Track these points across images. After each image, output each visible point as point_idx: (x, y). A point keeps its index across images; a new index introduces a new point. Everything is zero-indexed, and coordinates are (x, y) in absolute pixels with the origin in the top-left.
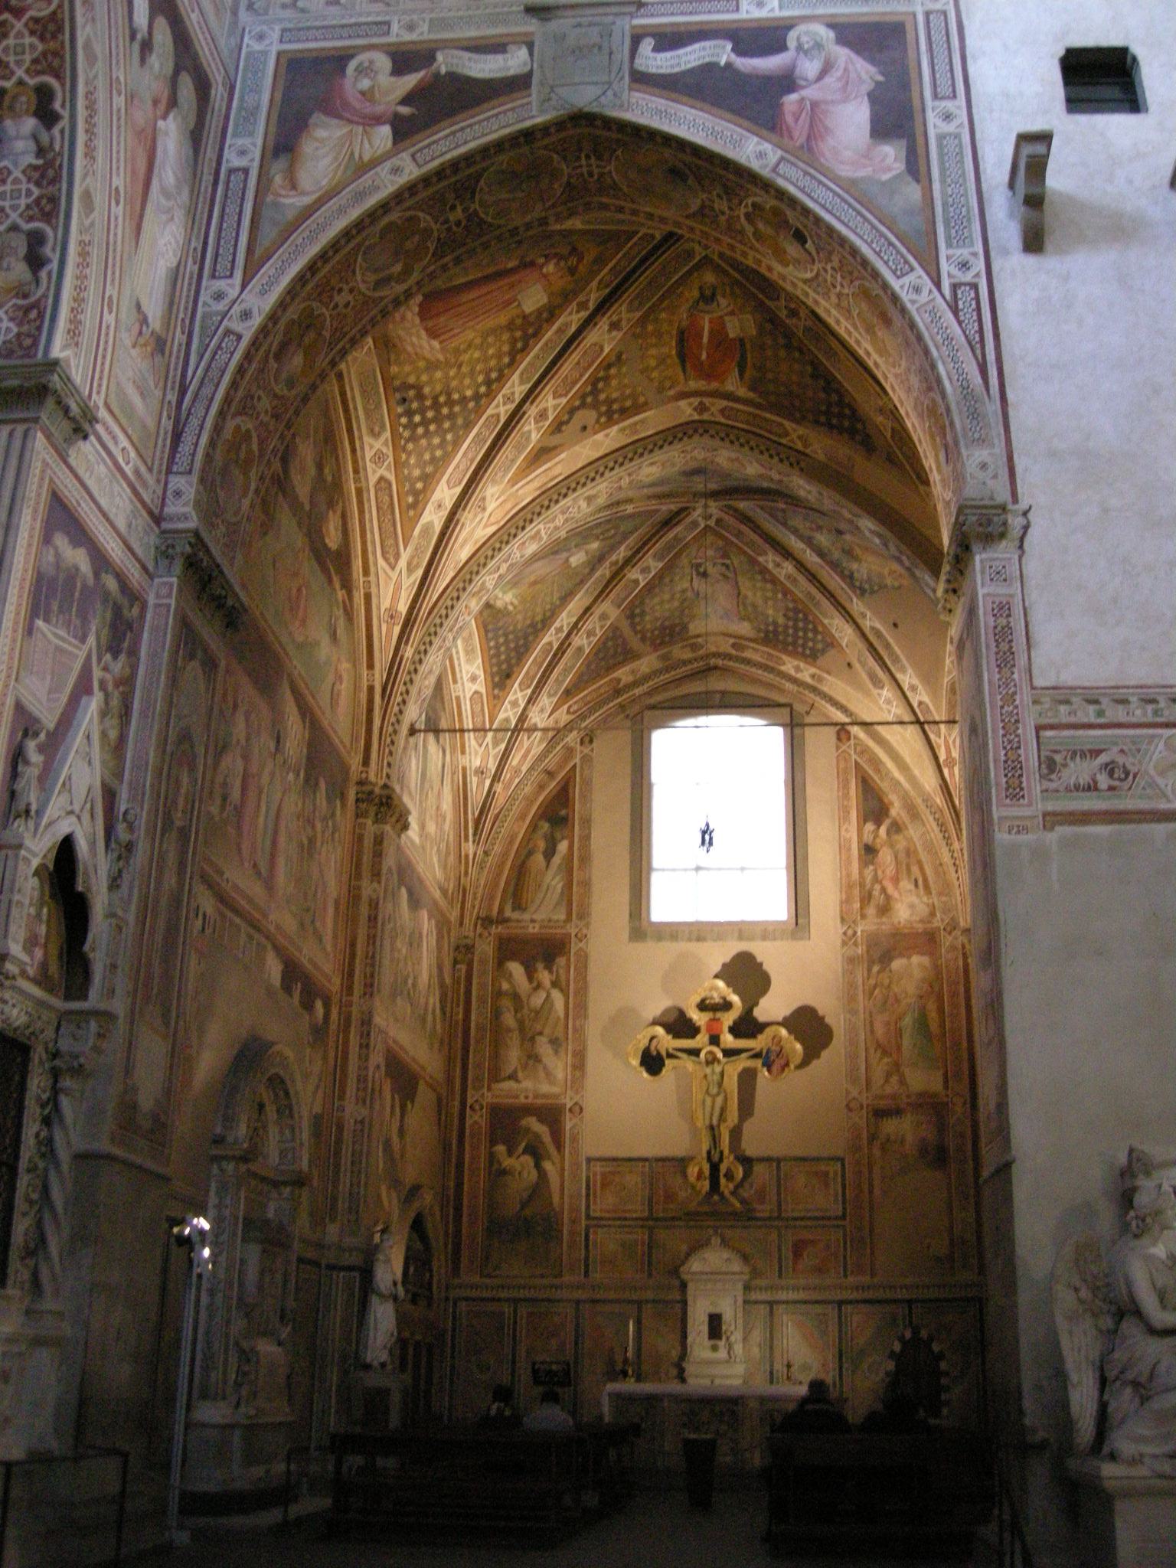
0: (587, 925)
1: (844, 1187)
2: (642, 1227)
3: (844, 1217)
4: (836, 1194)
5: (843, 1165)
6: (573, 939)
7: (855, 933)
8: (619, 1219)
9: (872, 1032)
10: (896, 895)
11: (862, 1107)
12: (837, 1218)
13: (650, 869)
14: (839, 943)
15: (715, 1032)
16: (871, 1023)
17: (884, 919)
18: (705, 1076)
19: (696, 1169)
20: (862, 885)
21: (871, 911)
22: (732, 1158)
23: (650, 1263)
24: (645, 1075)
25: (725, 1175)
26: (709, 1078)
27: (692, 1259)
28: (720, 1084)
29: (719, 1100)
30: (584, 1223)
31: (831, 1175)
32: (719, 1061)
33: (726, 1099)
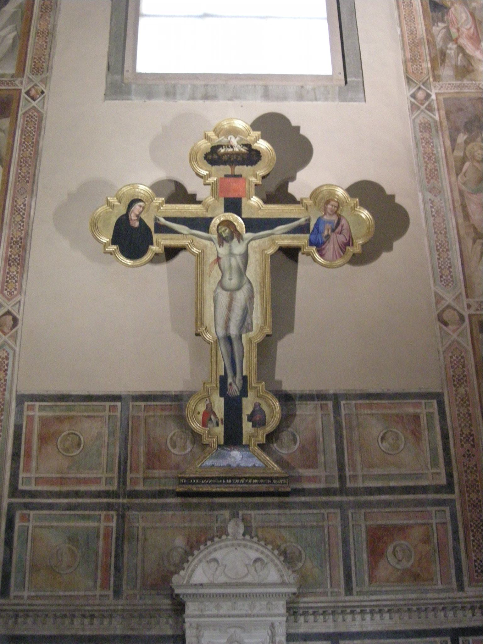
0: (45, 81)
1: (445, 437)
2: (109, 507)
3: (449, 487)
4: (433, 451)
5: (441, 404)
6: (23, 94)
7: (428, 96)
8: (68, 495)
9: (467, 216)
10: (477, 54)
11: (462, 318)
12: (438, 489)
13: (137, 15)
14: (406, 107)
15: (232, 195)
16: (464, 208)
17: (465, 82)
18: (218, 259)
19: (202, 408)
20: (431, 43)
21: (447, 72)
22: (261, 386)
23: (118, 569)
24: (122, 258)
25: (251, 418)
26: (224, 262)
27: (193, 561)
28: (242, 272)
29: (241, 296)
30: (6, 501)
31: (424, 420)
32: (240, 237)
33: (251, 298)
